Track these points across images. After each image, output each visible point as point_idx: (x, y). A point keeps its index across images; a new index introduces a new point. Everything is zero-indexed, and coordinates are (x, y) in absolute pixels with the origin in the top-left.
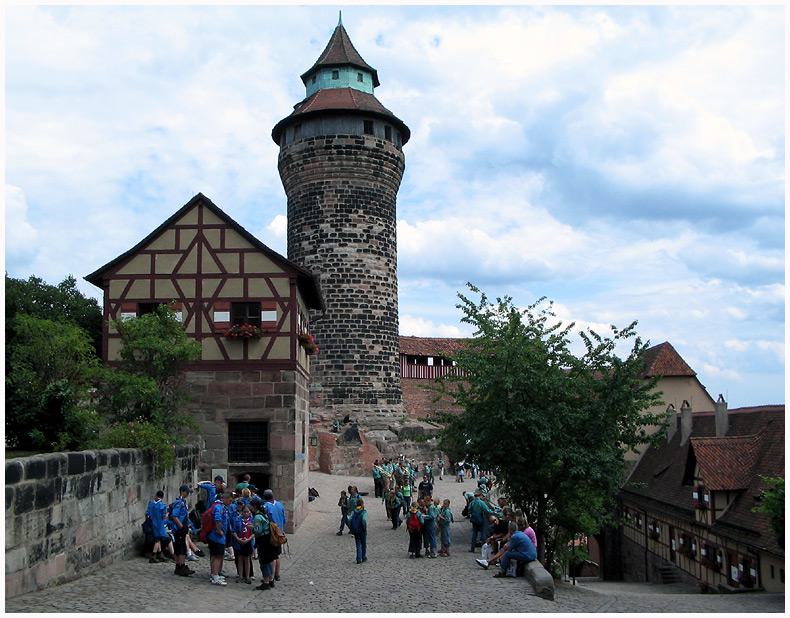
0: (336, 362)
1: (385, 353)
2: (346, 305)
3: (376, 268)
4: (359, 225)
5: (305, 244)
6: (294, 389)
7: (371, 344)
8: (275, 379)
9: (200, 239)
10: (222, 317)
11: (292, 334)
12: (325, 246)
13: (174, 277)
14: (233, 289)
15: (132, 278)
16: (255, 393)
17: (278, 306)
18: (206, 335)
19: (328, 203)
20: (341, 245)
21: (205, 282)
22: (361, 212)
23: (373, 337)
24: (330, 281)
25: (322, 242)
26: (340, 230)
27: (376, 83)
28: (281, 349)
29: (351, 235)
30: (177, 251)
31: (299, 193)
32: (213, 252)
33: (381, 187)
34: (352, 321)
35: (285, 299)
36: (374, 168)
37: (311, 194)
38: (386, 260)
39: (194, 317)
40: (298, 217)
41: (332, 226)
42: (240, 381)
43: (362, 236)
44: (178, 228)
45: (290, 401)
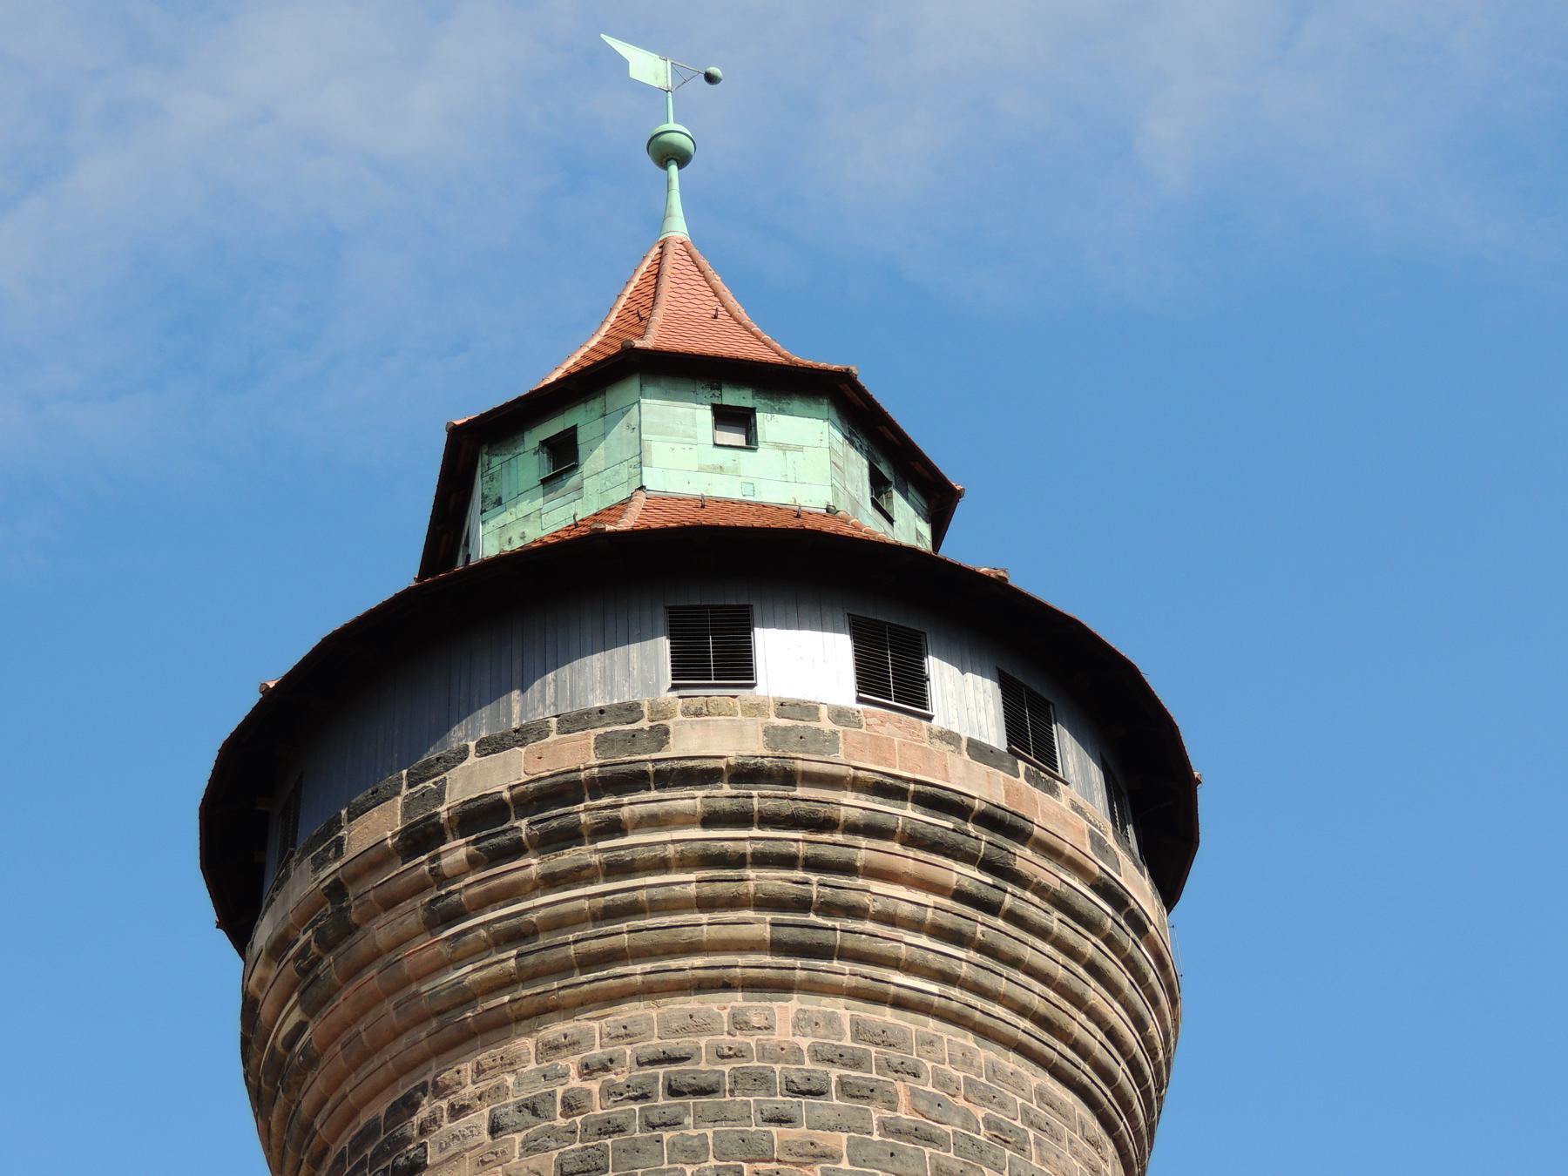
33: (859, 1030)
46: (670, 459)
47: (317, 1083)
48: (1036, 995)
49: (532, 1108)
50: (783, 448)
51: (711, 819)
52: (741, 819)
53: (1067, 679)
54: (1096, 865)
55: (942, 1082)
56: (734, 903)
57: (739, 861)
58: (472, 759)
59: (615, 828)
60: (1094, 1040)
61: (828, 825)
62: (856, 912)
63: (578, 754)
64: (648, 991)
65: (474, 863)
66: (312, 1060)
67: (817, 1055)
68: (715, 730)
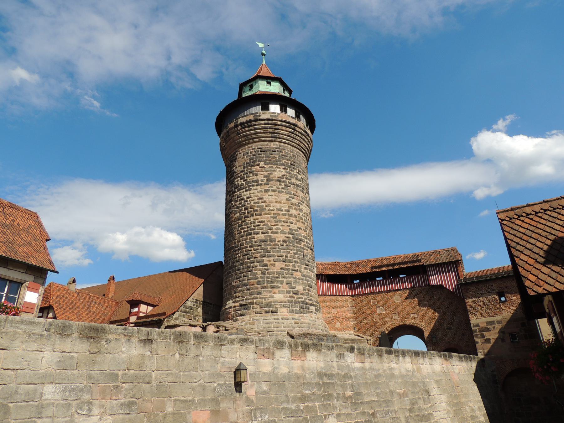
0: (242, 281)
1: (288, 269)
2: (250, 234)
3: (276, 202)
7: (272, 262)
19: (238, 167)
20: (246, 191)
23: (274, 256)
25: (235, 192)
29: (253, 182)
34: (255, 246)
41: (241, 179)
43: (262, 181)
46: (262, 87)
47: (227, 151)
48: (298, 142)
49: (247, 153)
51: (265, 124)
52: (268, 124)
53: (302, 110)
54: (304, 129)
56: (267, 133)
57: (267, 128)
59: (255, 125)
60: (303, 147)
61: (277, 125)
62: (279, 134)
63: (251, 117)
64: (259, 142)
65: (241, 129)
66: (226, 148)
68: (265, 115)
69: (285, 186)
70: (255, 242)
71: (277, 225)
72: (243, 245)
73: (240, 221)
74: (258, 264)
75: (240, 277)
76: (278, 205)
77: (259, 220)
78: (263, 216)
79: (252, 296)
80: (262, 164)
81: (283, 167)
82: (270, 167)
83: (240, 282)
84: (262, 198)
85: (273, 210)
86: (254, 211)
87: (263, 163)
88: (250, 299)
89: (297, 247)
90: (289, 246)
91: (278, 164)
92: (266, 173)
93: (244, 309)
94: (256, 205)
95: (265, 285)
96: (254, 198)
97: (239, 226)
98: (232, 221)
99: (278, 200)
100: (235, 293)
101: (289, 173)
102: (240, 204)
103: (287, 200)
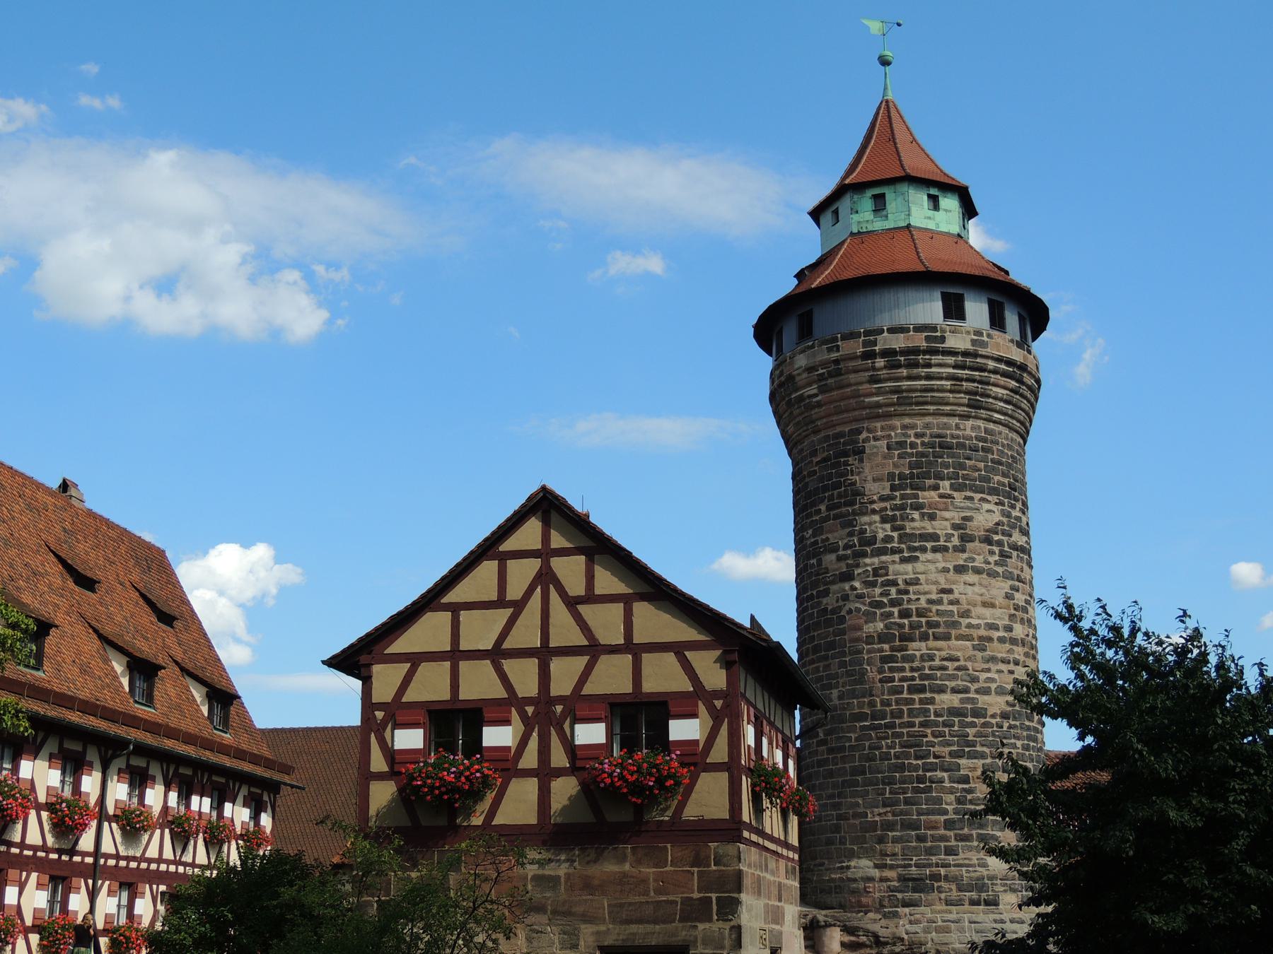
0: (901, 813)
2: (922, 689)
4: (947, 514)
5: (830, 559)
6: (737, 881)
8: (698, 861)
9: (546, 578)
10: (591, 734)
11: (732, 767)
12: (871, 562)
13: (497, 654)
14: (612, 677)
15: (415, 660)
16: (659, 891)
17: (702, 709)
18: (560, 772)
19: (872, 478)
20: (904, 560)
21: (556, 665)
22: (945, 485)
24: (883, 638)
25: (865, 555)
26: (902, 528)
27: (969, 211)
28: (708, 798)
30: (500, 603)
31: (814, 453)
32: (572, 603)
33: (986, 430)
35: (716, 694)
36: (967, 392)
37: (838, 455)
38: (1006, 585)
39: (535, 734)
40: (814, 504)
41: (884, 520)
42: (627, 867)
44: (503, 558)
45: (730, 907)
49: (901, 444)
50: (946, 211)
51: (955, 367)
52: (963, 367)
55: (1003, 446)
56: (959, 392)
57: (961, 380)
58: (885, 334)
59: (929, 365)
62: (989, 396)
65: (885, 367)
67: (976, 438)
69: (1002, 554)
70: (937, 715)
71: (989, 670)
72: (901, 717)
73: (886, 647)
74: (945, 775)
75: (896, 803)
76: (987, 612)
77: (944, 654)
78: (953, 642)
79: (934, 859)
80: (945, 485)
81: (994, 499)
82: (967, 498)
83: (894, 815)
84: (950, 591)
85: (978, 627)
86: (930, 625)
87: (947, 484)
88: (930, 865)
89: (1029, 728)
90: (1015, 727)
91: (984, 487)
92: (955, 516)
93: (915, 890)
94: (934, 608)
95: (966, 831)
96: (926, 588)
97: (885, 660)
98: (858, 640)
99: (987, 598)
100: (881, 840)
101: (1009, 516)
102: (881, 594)
103: (1009, 597)
